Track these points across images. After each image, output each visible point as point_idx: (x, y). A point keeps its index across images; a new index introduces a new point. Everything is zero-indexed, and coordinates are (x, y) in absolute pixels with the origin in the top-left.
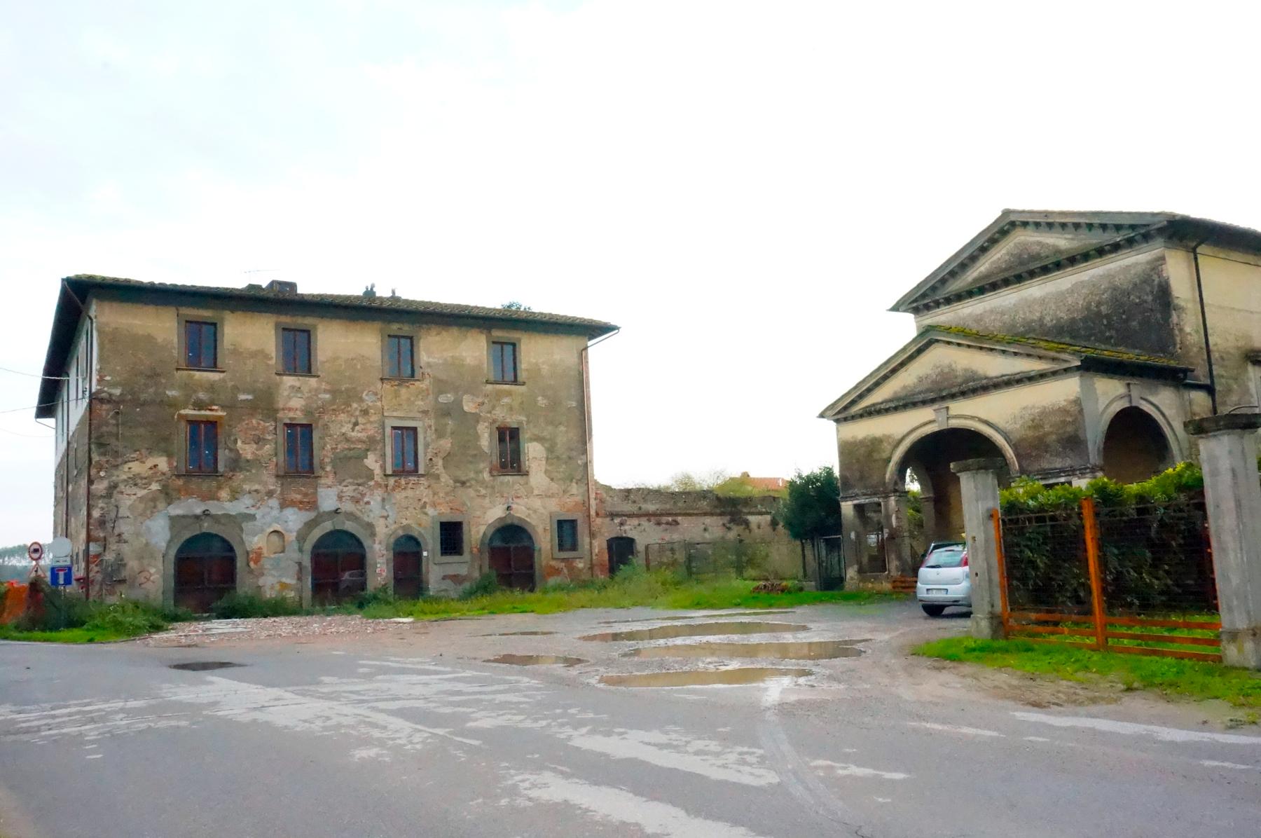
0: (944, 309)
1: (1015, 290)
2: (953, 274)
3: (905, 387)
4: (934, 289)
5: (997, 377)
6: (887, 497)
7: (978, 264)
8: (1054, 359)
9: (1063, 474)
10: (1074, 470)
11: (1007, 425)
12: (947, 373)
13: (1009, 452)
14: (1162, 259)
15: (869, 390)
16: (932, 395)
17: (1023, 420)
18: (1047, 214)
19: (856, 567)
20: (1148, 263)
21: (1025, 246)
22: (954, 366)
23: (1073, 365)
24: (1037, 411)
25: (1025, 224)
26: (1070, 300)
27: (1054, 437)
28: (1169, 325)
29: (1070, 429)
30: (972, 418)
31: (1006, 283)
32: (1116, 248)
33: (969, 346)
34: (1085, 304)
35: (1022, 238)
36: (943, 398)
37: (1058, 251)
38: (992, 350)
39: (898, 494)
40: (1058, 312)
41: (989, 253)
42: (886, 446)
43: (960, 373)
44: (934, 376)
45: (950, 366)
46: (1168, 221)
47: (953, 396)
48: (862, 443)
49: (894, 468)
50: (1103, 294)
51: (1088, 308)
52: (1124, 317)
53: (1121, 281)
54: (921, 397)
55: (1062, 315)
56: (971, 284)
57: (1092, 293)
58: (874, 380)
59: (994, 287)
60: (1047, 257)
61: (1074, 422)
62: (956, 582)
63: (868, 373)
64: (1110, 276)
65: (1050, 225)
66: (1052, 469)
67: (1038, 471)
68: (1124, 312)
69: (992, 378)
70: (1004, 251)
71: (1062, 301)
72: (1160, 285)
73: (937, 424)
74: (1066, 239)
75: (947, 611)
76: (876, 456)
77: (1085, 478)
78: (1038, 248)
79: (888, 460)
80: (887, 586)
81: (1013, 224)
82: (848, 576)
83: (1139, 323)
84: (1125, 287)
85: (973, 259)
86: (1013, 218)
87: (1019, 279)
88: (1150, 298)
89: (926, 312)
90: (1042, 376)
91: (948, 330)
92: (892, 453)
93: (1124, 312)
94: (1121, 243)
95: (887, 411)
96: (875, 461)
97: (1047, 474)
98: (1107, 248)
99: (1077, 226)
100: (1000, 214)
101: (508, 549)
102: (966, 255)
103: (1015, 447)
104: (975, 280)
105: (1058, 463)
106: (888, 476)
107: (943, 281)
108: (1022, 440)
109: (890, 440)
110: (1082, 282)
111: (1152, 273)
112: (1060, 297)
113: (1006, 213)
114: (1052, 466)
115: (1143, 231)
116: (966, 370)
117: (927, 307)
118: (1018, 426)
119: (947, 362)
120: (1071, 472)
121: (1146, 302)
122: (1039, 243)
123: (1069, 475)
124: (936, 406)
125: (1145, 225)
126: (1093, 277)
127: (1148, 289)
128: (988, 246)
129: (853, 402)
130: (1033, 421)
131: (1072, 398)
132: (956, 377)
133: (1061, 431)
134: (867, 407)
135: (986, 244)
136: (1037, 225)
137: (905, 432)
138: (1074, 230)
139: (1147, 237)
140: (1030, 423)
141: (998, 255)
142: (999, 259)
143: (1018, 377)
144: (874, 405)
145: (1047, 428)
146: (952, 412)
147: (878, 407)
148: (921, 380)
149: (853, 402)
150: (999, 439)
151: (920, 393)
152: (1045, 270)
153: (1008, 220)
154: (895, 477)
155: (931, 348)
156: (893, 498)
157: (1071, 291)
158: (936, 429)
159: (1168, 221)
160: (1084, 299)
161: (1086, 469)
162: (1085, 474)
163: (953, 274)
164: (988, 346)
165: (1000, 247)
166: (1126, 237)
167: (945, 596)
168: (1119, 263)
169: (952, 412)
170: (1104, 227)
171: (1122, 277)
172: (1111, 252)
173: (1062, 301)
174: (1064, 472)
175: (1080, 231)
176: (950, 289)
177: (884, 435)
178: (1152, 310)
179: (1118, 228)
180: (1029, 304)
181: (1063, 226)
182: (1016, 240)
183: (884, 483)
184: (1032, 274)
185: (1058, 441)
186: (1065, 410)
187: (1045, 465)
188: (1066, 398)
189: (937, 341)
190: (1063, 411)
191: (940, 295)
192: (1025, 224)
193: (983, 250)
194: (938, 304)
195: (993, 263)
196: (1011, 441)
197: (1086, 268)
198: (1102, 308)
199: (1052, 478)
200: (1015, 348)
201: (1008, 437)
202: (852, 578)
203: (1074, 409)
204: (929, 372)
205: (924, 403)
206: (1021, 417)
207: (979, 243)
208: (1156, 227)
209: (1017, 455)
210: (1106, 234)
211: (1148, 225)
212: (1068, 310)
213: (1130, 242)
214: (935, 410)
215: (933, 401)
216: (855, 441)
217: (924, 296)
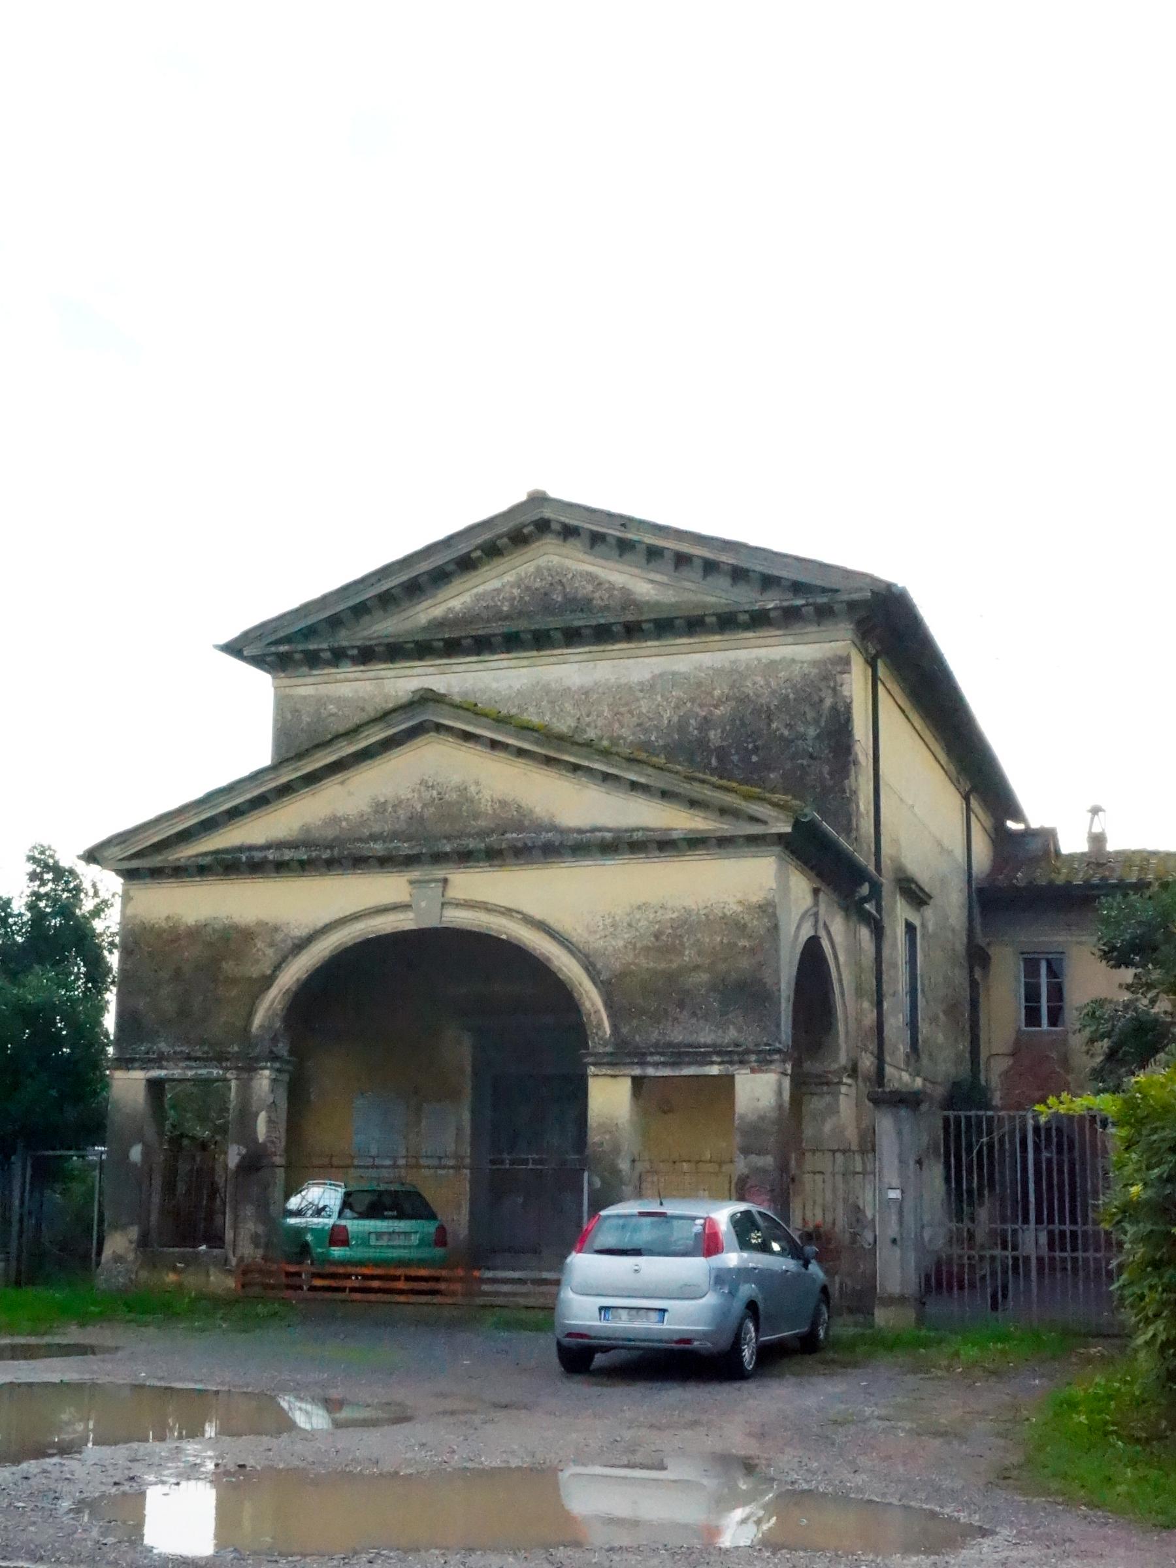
0: (348, 670)
1: (525, 662)
2: (387, 600)
3: (334, 820)
4: (335, 622)
5: (580, 831)
6: (249, 1067)
7: (442, 594)
8: (724, 811)
9: (715, 1058)
10: (748, 1052)
11: (591, 939)
12: (450, 804)
13: (591, 998)
14: (844, 662)
15: (235, 814)
16: (406, 848)
17: (633, 933)
18: (626, 522)
19: (134, 1232)
20: (814, 663)
21: (558, 579)
22: (473, 789)
23: (774, 830)
24: (670, 915)
25: (569, 532)
26: (644, 706)
27: (705, 977)
28: (844, 792)
29: (744, 963)
30: (508, 912)
31: (512, 642)
32: (759, 620)
33: (521, 753)
34: (675, 719)
35: (556, 560)
36: (438, 858)
37: (629, 601)
38: (576, 768)
39: (277, 1065)
40: (616, 725)
41: (474, 574)
42: (264, 955)
43: (486, 806)
44: (419, 808)
45: (462, 790)
46: (872, 592)
47: (465, 857)
48: (195, 933)
49: (278, 1006)
50: (716, 707)
51: (682, 727)
52: (754, 759)
53: (754, 685)
54: (378, 848)
55: (625, 732)
56: (425, 629)
57: (693, 700)
58: (256, 793)
59: (481, 645)
60: (607, 608)
61: (753, 951)
62: (686, 1292)
63: (245, 772)
64: (736, 675)
65: (624, 547)
66: (691, 1046)
67: (656, 1045)
68: (756, 749)
69: (570, 830)
70: (509, 578)
71: (627, 704)
72: (834, 708)
73: (411, 915)
74: (652, 581)
75: (599, 1359)
76: (228, 967)
77: (766, 1071)
78: (590, 588)
79: (267, 981)
80: (221, 1282)
81: (543, 526)
82: (107, 1252)
83: (783, 776)
84: (763, 701)
85: (440, 577)
86: (548, 513)
87: (541, 641)
88: (812, 732)
89: (305, 670)
90: (695, 843)
91: (470, 709)
92: (278, 968)
93: (756, 749)
94: (772, 614)
95: (281, 867)
96: (233, 981)
97: (680, 1054)
98: (743, 618)
99: (682, 560)
100: (523, 498)
101: (1001, 1223)
102: (425, 566)
103: (607, 989)
104: (439, 624)
105: (706, 1036)
106: (258, 1020)
107: (360, 610)
108: (623, 975)
109: (279, 937)
110: (674, 674)
111: (822, 685)
112: (623, 695)
113: (538, 499)
114: (692, 1039)
115: (822, 600)
116: (503, 804)
117: (313, 660)
118: (621, 943)
119: (456, 779)
120: (736, 1055)
121: (803, 737)
122: (591, 578)
123: (731, 1063)
124: (416, 874)
125: (824, 590)
126: (699, 668)
127: (810, 715)
128: (479, 559)
129: (185, 836)
130: (657, 936)
131: (756, 898)
132: (476, 816)
133: (722, 967)
134: (226, 851)
135: (478, 553)
136: (596, 539)
137: (320, 924)
138: (671, 567)
139: (824, 614)
140: (649, 941)
141: (496, 584)
142: (498, 591)
143: (637, 836)
144: (240, 849)
145: (689, 955)
146: (454, 893)
147: (258, 855)
148: (380, 808)
149: (185, 836)
150: (568, 967)
151: (373, 838)
152: (602, 635)
153: (534, 515)
154: (278, 1025)
155: (419, 741)
156: (267, 1073)
157: (649, 688)
158: (410, 925)
159: (872, 592)
160: (677, 707)
161: (770, 1052)
162: (771, 1062)
163: (387, 600)
164: (572, 759)
165: (502, 568)
166: (785, 604)
167: (658, 1326)
168: (732, 655)
169: (454, 893)
170: (739, 575)
171: (761, 681)
172: (747, 627)
173: (627, 704)
174: (719, 1053)
175: (685, 572)
176: (376, 628)
177: (262, 924)
178: (811, 757)
179: (768, 582)
180: (555, 696)
181: (653, 554)
182: (542, 562)
183: (246, 1028)
184: (572, 637)
185: (713, 988)
186: (737, 923)
187: (677, 1035)
188: (740, 896)
189: (439, 728)
190: (736, 926)
191: (345, 638)
192: (569, 532)
193: (466, 564)
194: (338, 656)
195: (479, 598)
196: (599, 973)
197: (622, 654)
198: (712, 734)
199: (690, 1064)
200: (640, 774)
201: (593, 965)
202: (118, 1259)
203: (758, 924)
204: (405, 794)
205: (385, 862)
206: (630, 925)
207: (462, 549)
208: (845, 597)
209: (609, 1005)
210: (736, 590)
211: (837, 591)
212: (639, 725)
213: (789, 617)
214: (411, 882)
215: (410, 861)
216: (174, 928)
217: (309, 632)
